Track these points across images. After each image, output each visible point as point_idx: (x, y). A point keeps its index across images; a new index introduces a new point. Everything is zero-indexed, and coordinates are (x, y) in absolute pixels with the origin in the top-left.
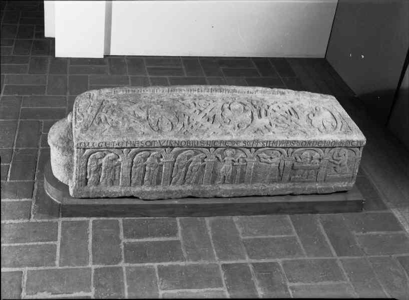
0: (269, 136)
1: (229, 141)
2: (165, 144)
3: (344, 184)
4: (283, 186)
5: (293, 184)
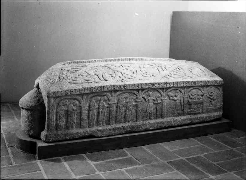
0: (171, 80)
1: (150, 83)
2: (110, 89)
3: (217, 113)
5: (190, 116)
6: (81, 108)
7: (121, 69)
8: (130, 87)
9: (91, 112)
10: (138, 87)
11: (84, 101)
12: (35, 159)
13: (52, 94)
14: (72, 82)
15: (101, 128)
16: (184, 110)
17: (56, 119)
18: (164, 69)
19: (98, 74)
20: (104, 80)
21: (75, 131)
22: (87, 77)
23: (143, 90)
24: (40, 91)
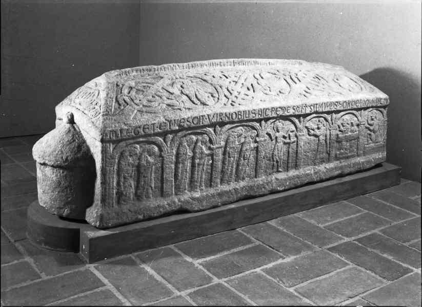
1: (280, 108)
2: (214, 120)
3: (379, 155)
4: (331, 165)
5: (339, 161)
6: (163, 160)
8: (247, 116)
9: (181, 166)
10: (261, 115)
11: (169, 145)
12: (83, 263)
13: (110, 134)
14: (144, 109)
15: (197, 195)
16: (330, 151)
17: (118, 184)
19: (187, 92)
20: (201, 103)
21: (154, 203)
22: (168, 99)
24: (77, 129)
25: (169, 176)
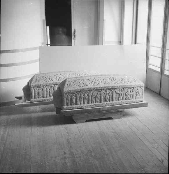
0: (117, 85)
7: (94, 81)
18: (115, 80)
23: (103, 89)
25: (78, 100)
